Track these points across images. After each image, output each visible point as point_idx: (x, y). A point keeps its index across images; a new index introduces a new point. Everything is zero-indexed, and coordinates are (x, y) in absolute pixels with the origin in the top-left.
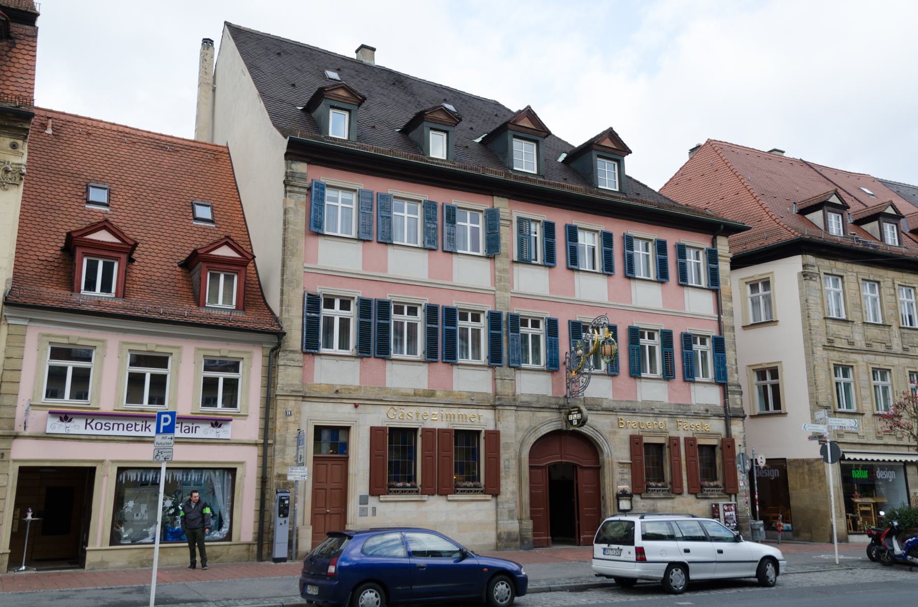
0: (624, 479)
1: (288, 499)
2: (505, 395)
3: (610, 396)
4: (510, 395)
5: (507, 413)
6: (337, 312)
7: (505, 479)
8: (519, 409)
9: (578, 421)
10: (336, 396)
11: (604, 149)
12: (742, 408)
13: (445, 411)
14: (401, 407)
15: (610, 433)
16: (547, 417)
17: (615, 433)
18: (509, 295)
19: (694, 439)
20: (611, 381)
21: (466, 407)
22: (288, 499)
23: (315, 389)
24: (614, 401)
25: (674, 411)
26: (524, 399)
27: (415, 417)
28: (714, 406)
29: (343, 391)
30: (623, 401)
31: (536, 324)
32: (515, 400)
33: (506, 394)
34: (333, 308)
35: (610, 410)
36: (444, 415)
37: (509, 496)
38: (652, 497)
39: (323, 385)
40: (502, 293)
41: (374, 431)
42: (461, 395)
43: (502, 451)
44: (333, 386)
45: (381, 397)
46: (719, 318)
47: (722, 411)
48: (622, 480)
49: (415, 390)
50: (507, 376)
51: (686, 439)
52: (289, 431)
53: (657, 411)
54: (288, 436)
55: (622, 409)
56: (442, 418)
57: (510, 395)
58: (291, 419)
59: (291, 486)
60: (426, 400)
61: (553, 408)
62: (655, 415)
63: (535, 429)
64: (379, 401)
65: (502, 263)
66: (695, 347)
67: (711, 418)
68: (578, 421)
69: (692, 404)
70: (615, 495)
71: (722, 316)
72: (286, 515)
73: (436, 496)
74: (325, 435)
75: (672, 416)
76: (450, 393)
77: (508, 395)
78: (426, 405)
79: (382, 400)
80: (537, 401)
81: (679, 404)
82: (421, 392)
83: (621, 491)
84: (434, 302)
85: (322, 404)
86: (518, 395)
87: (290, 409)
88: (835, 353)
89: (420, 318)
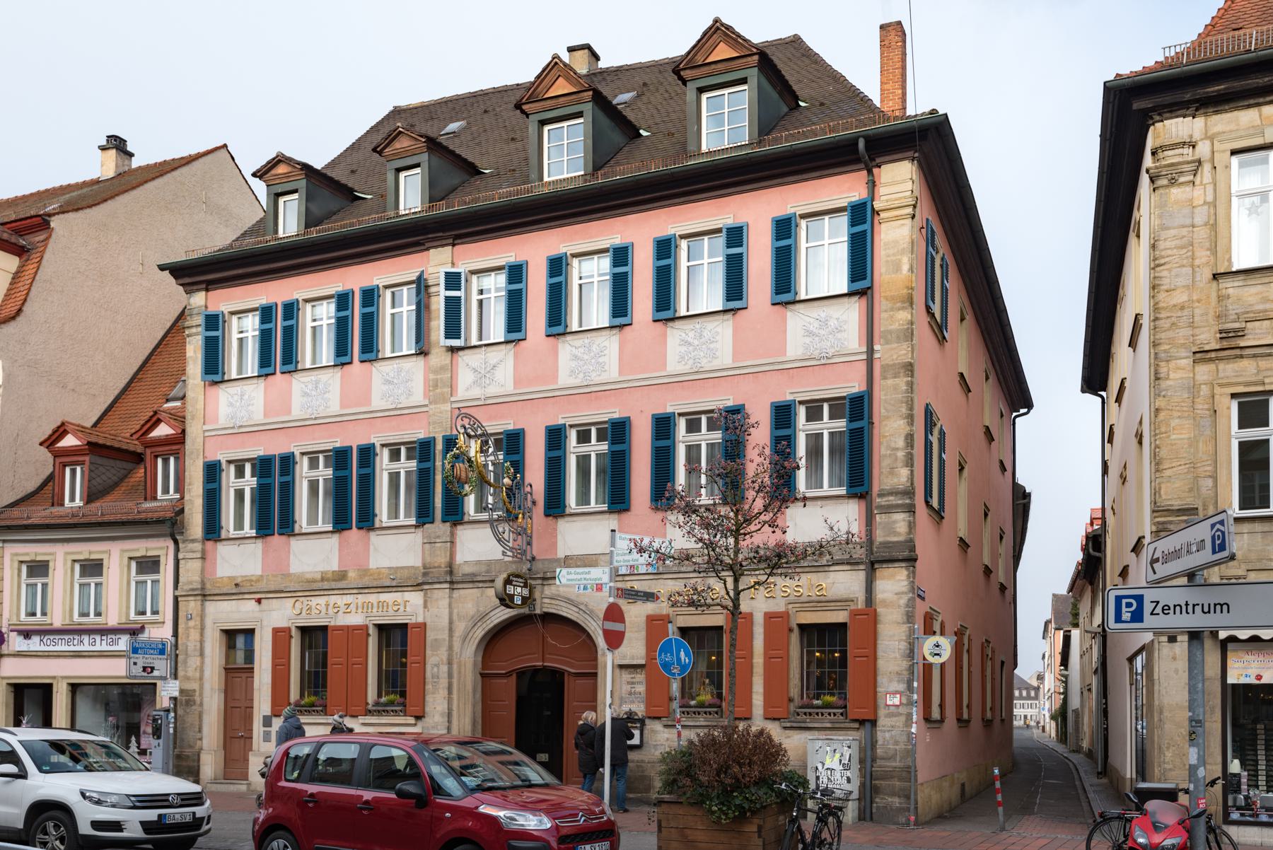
0: (635, 693)
2: (435, 567)
4: (443, 566)
5: (437, 594)
6: (248, 481)
7: (433, 693)
8: (455, 586)
9: (511, 597)
10: (238, 590)
12: (911, 541)
13: (361, 599)
18: (447, 407)
19: (785, 616)
21: (386, 590)
26: (467, 570)
27: (324, 611)
29: (244, 583)
32: (451, 573)
33: (436, 565)
36: (360, 604)
40: (438, 406)
42: (379, 574)
43: (428, 652)
45: (281, 587)
46: (870, 351)
47: (859, 553)
48: (630, 694)
49: (322, 573)
50: (438, 537)
51: (769, 617)
54: (189, 644)
56: (357, 609)
57: (443, 566)
58: (191, 623)
60: (333, 585)
64: (279, 593)
65: (438, 357)
67: (832, 568)
68: (511, 597)
72: (159, 738)
76: (365, 572)
77: (440, 567)
78: (336, 592)
80: (487, 572)
82: (330, 575)
83: (626, 713)
84: (347, 444)
85: (226, 603)
86: (460, 565)
88: (1245, 363)
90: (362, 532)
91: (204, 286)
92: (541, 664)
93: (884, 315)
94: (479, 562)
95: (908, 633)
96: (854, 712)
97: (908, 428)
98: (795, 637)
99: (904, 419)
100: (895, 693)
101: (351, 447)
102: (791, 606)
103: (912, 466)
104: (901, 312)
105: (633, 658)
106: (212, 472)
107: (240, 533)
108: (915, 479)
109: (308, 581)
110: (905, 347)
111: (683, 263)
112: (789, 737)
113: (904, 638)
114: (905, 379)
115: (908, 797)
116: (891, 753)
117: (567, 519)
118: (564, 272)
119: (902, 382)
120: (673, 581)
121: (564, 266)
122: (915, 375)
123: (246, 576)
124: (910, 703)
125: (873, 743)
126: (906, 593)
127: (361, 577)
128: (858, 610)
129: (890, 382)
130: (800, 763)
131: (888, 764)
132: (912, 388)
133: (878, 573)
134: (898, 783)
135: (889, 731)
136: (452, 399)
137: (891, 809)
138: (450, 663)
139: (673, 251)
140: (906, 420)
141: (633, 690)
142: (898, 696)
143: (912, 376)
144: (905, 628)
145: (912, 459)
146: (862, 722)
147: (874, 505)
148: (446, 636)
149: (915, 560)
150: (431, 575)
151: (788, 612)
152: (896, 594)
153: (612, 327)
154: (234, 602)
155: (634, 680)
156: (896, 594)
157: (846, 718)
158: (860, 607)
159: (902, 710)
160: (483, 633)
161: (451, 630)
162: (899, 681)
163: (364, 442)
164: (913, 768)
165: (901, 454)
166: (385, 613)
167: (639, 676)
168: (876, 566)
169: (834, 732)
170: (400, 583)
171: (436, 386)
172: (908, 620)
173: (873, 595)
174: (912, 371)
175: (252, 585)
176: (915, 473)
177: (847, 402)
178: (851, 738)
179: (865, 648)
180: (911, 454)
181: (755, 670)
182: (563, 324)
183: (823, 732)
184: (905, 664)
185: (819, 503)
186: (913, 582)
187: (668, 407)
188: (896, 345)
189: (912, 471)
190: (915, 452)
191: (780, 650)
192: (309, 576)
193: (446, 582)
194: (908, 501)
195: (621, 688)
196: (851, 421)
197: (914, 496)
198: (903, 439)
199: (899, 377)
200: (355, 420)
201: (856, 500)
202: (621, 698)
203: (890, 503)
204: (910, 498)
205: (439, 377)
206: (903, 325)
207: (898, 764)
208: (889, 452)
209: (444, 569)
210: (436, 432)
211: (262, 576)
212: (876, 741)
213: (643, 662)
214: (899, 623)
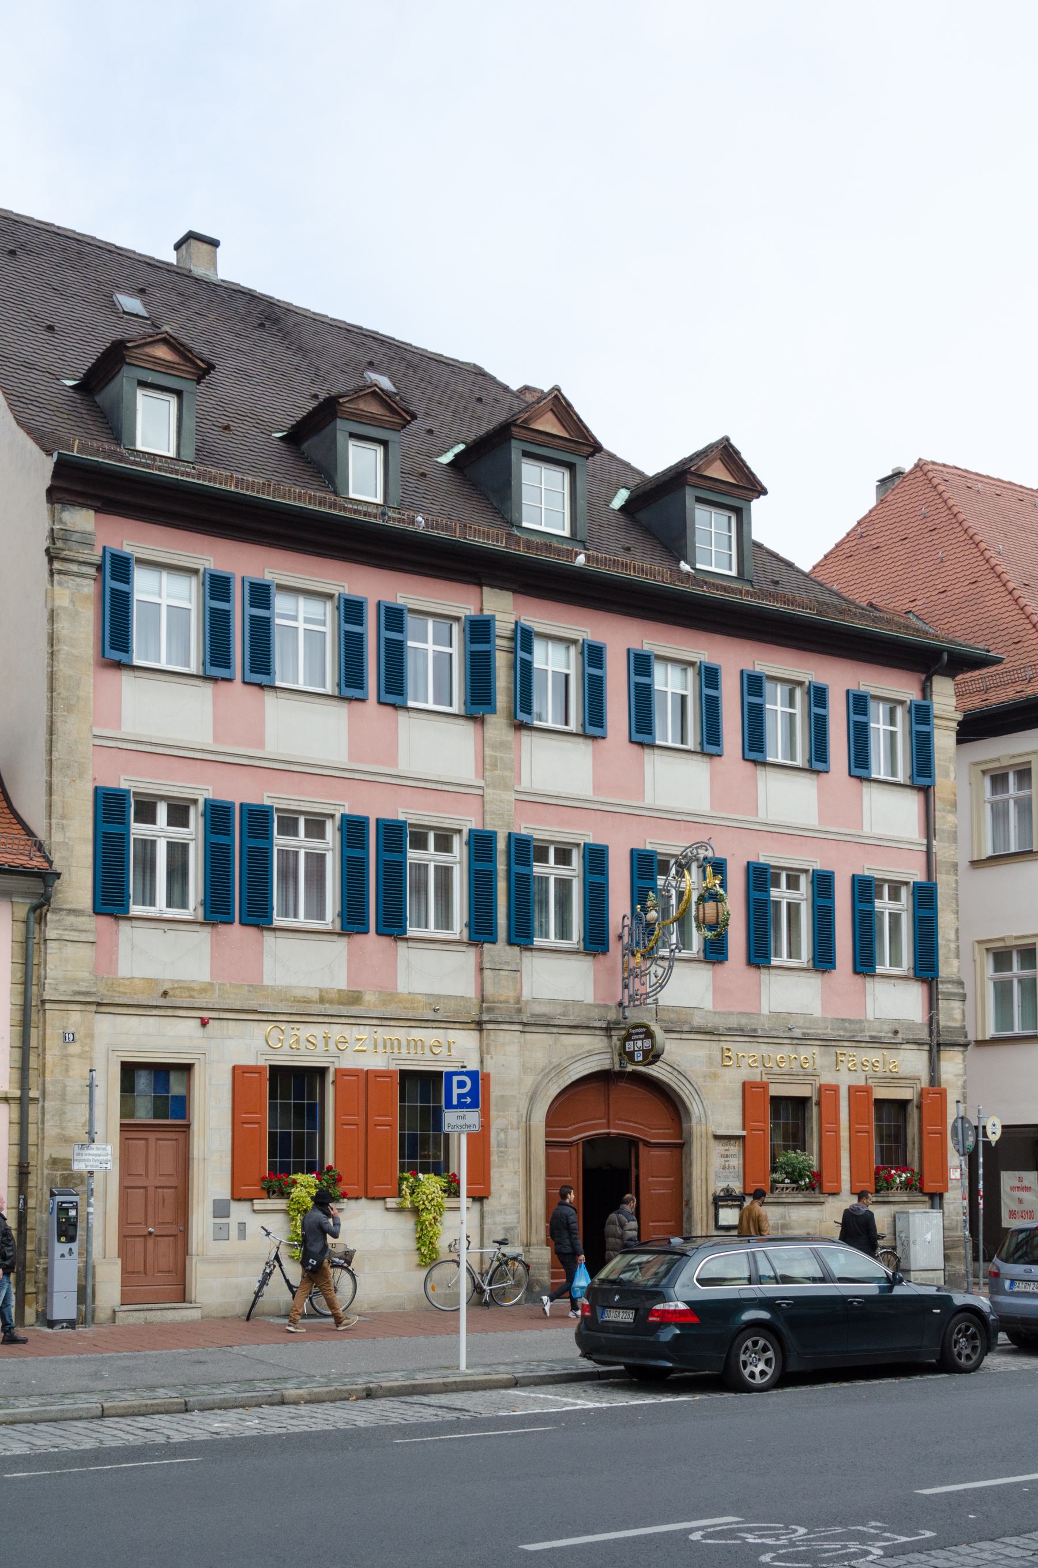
1: (76, 1208)
2: (501, 1002)
3: (708, 1004)
6: (162, 830)
7: (499, 1167)
8: (527, 1029)
9: (646, 1053)
12: (964, 1027)
13: (383, 1033)
14: (292, 1025)
15: (705, 1077)
16: (583, 1046)
17: (715, 1076)
19: (867, 1090)
20: (710, 973)
21: (423, 1024)
22: (76, 1208)
23: (122, 990)
24: (715, 1013)
25: (830, 1033)
26: (538, 1009)
27: (321, 1045)
28: (910, 1025)
29: (178, 992)
30: (732, 1014)
31: (563, 857)
32: (519, 1011)
33: (502, 999)
34: (153, 821)
35: (709, 1033)
36: (380, 1042)
37: (506, 1199)
38: (781, 1200)
39: (136, 981)
41: (239, 1073)
44: (156, 982)
45: (253, 1005)
47: (924, 1035)
48: (724, 1168)
49: (321, 990)
50: (507, 963)
51: (852, 1090)
52: (71, 1073)
53: (797, 1033)
55: (730, 1029)
56: (375, 1048)
57: (512, 1001)
58: (74, 1049)
59: (78, 1181)
60: (344, 1010)
61: (595, 1028)
62: (795, 1042)
63: (559, 1069)
66: (878, 904)
67: (903, 1046)
68: (646, 1053)
69: (867, 1020)
70: (711, 1198)
71: (935, 843)
72: (71, 1239)
73: (363, 1201)
74: (143, 1081)
75: (826, 1042)
76: (390, 996)
77: (507, 1002)
78: (343, 1020)
79: (255, 1012)
81: (842, 1020)
82: (334, 996)
83: (723, 1190)
84: (359, 812)
86: (527, 1002)
87: (72, 1030)
89: (331, 843)
90: (385, 941)
94: (551, 1001)
101: (367, 819)
104: (950, 815)
105: (728, 1127)
109: (297, 1000)
116: (954, 1223)
120: (767, 1045)
123: (178, 981)
127: (384, 1003)
141: (727, 1164)
154: (152, 1019)
155: (727, 1153)
167: (732, 1148)
170: (448, 1017)
175: (191, 997)
185: (893, 981)
192: (299, 993)
200: (370, 780)
205: (498, 754)
211: (211, 984)
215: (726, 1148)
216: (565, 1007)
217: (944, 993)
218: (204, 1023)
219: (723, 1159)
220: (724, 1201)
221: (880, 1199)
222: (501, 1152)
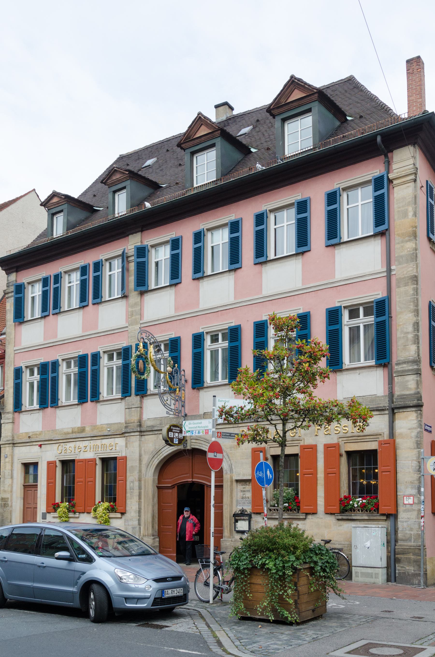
2: (131, 423)
7: (130, 499)
8: (143, 434)
9: (172, 439)
11: (295, 104)
12: (418, 393)
13: (93, 443)
15: (231, 448)
18: (137, 327)
21: (106, 437)
26: (149, 423)
27: (73, 451)
28: (374, 398)
32: (140, 426)
33: (132, 421)
36: (92, 447)
38: (273, 517)
40: (133, 327)
42: (102, 428)
43: (128, 474)
46: (389, 270)
48: (243, 498)
50: (133, 404)
51: (327, 447)
54: (6, 472)
56: (90, 449)
57: (136, 422)
58: (7, 460)
68: (172, 439)
73: (85, 514)
76: (94, 427)
77: (134, 422)
79: (52, 440)
82: (76, 430)
83: (240, 511)
86: (145, 421)
90: (93, 404)
91: (15, 270)
92: (191, 480)
93: (397, 246)
95: (417, 455)
96: (383, 509)
97: (415, 319)
98: (344, 460)
99: (412, 312)
100: (409, 496)
101: (87, 354)
102: (341, 440)
103: (418, 343)
104: (408, 243)
105: (244, 475)
106: (18, 373)
107: (32, 408)
108: (421, 352)
110: (411, 265)
111: (272, 227)
112: (341, 526)
113: (415, 459)
114: (412, 287)
115: (419, 566)
116: (408, 536)
117: (205, 390)
118: (202, 240)
119: (410, 289)
121: (202, 237)
122: (419, 283)
123: (34, 432)
124: (419, 503)
125: (396, 531)
126: (415, 428)
127: (92, 430)
128: (384, 441)
129: (402, 289)
130: (347, 543)
131: (406, 544)
132: (417, 292)
133: (397, 416)
134: (412, 557)
135: (406, 521)
136: (141, 322)
137: (409, 575)
138: (140, 480)
139: (265, 220)
140: (413, 314)
141: (244, 496)
142: (412, 498)
143: (417, 284)
144: (415, 452)
145: (418, 339)
146: (388, 516)
147: (394, 371)
148: (137, 464)
149: (422, 406)
150: (129, 428)
151: (339, 444)
152: (409, 429)
153: (230, 271)
155: (244, 489)
156: (409, 429)
157: (378, 513)
158: (385, 439)
159: (415, 507)
160: (158, 461)
161: (140, 460)
162: (412, 488)
163: (94, 351)
164: (422, 546)
165: (410, 336)
166: (105, 451)
167: (247, 486)
168: (395, 411)
169: (370, 522)
171: (132, 315)
172: (417, 446)
173: (394, 430)
174: (417, 281)
175: (37, 437)
176: (421, 348)
177: (374, 304)
178: (380, 526)
179: (388, 466)
180: (418, 336)
181: (319, 482)
182: (202, 272)
183: (363, 522)
184: (416, 476)
185: (358, 371)
186: (420, 420)
187: (263, 316)
188: (406, 265)
189: (418, 347)
190: (420, 334)
191: (334, 468)
192: (65, 431)
193: (137, 431)
194: (416, 367)
195: (237, 495)
196: (377, 317)
197: (420, 363)
198: (412, 326)
199: (408, 285)
201: (382, 368)
202: (237, 501)
203: (404, 369)
204: (417, 365)
205: (134, 309)
206: (410, 251)
207: (412, 544)
208: (403, 335)
209: (137, 424)
210: (132, 342)
211: (42, 431)
212: (398, 528)
213: (250, 478)
214: (411, 449)
215: (244, 487)
216: (161, 420)
217: (398, 372)
218: (40, 446)
219: (242, 493)
220: (238, 517)
221: (344, 517)
222: (131, 492)
